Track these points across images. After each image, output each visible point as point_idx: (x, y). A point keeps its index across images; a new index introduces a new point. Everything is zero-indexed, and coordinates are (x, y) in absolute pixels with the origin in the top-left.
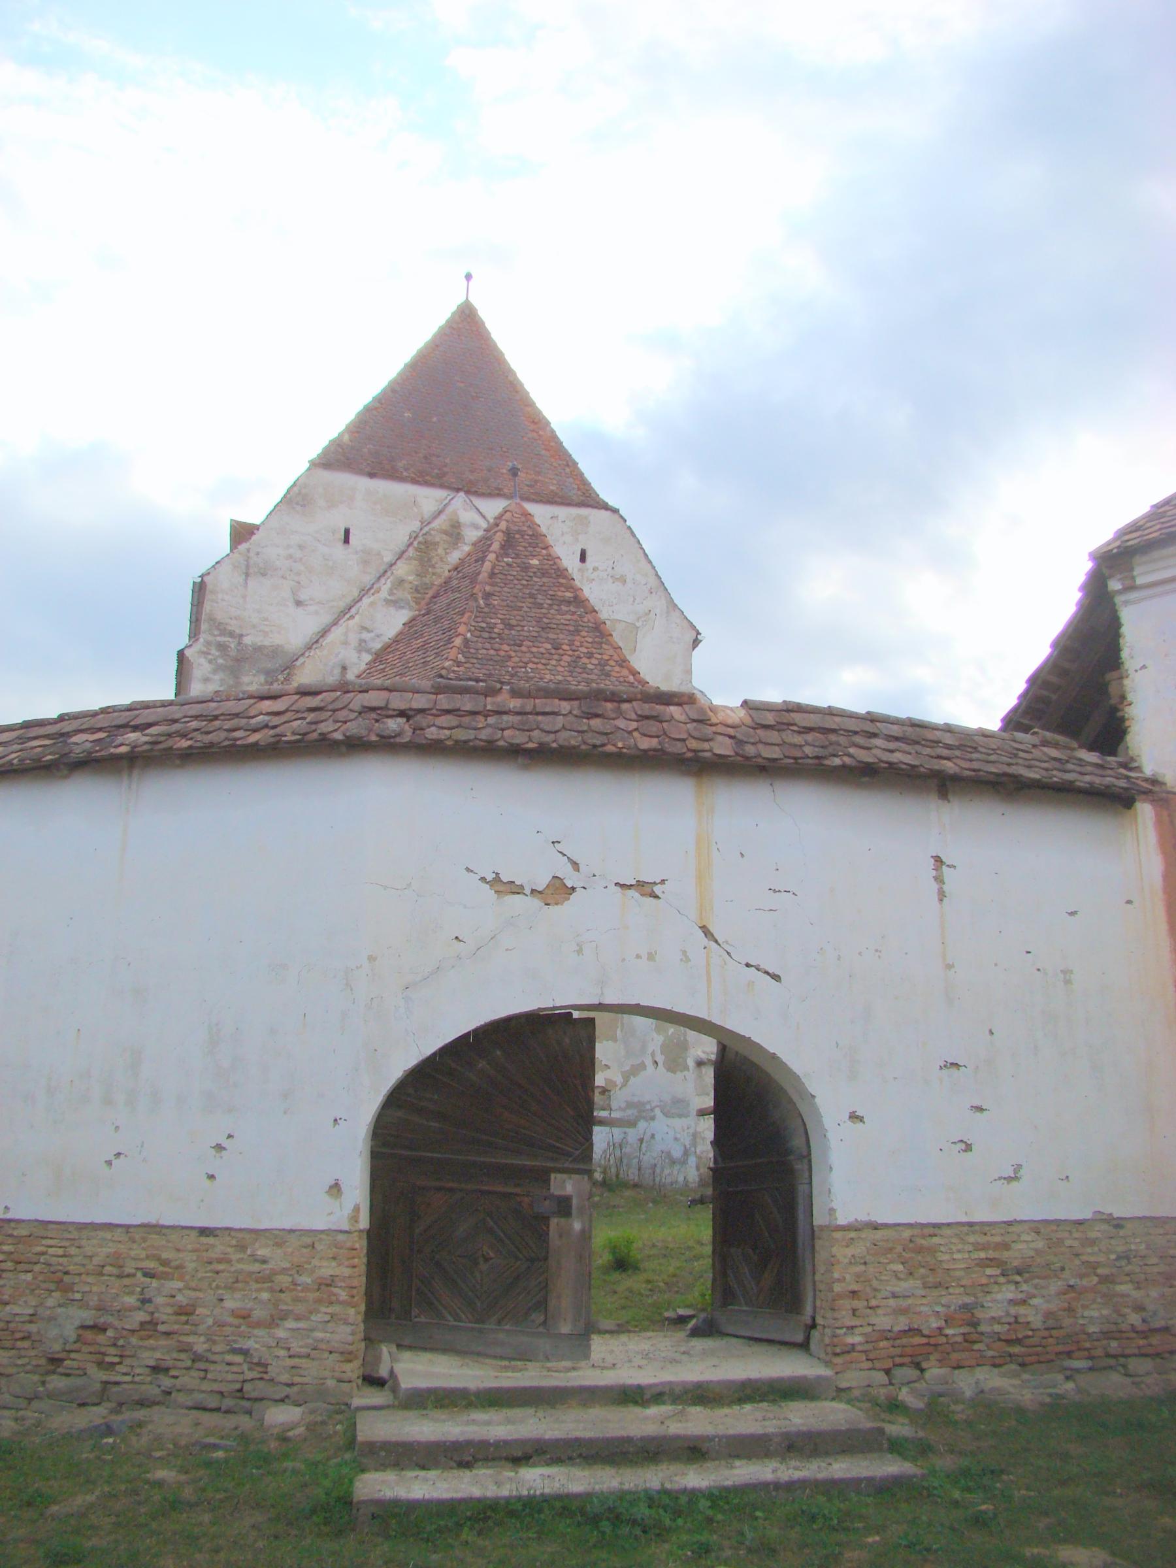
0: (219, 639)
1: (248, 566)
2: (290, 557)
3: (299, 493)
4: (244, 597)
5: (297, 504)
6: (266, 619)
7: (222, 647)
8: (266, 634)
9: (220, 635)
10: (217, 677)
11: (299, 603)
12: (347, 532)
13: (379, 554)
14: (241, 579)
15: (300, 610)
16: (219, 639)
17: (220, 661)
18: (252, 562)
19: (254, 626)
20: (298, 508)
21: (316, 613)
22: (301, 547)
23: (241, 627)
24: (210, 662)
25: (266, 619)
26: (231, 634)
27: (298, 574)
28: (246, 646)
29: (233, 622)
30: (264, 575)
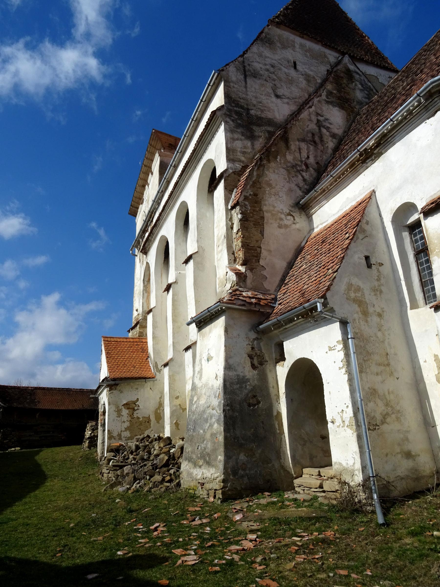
0: (235, 109)
1: (245, 71)
2: (267, 70)
3: (266, 37)
4: (246, 87)
5: (266, 42)
6: (261, 103)
7: (238, 114)
8: (262, 111)
9: (236, 107)
10: (239, 130)
11: (277, 96)
12: (295, 63)
13: (314, 77)
14: (242, 77)
15: (279, 101)
16: (235, 109)
17: (239, 122)
18: (247, 69)
19: (254, 106)
20: (267, 45)
21: (288, 103)
22: (273, 66)
23: (247, 105)
24: (233, 121)
25: (261, 103)
26: (242, 107)
27: (274, 80)
28: (252, 115)
29: (241, 100)
30: (255, 77)
